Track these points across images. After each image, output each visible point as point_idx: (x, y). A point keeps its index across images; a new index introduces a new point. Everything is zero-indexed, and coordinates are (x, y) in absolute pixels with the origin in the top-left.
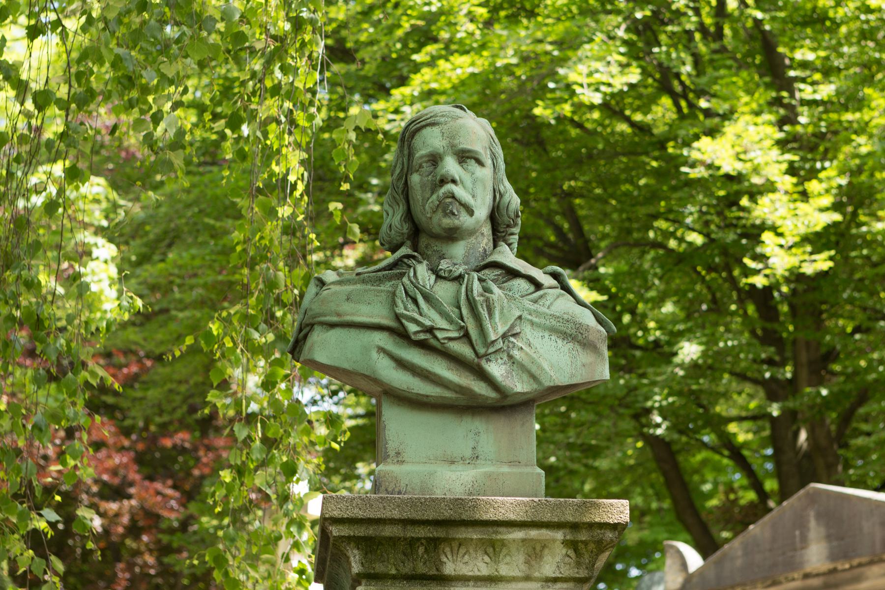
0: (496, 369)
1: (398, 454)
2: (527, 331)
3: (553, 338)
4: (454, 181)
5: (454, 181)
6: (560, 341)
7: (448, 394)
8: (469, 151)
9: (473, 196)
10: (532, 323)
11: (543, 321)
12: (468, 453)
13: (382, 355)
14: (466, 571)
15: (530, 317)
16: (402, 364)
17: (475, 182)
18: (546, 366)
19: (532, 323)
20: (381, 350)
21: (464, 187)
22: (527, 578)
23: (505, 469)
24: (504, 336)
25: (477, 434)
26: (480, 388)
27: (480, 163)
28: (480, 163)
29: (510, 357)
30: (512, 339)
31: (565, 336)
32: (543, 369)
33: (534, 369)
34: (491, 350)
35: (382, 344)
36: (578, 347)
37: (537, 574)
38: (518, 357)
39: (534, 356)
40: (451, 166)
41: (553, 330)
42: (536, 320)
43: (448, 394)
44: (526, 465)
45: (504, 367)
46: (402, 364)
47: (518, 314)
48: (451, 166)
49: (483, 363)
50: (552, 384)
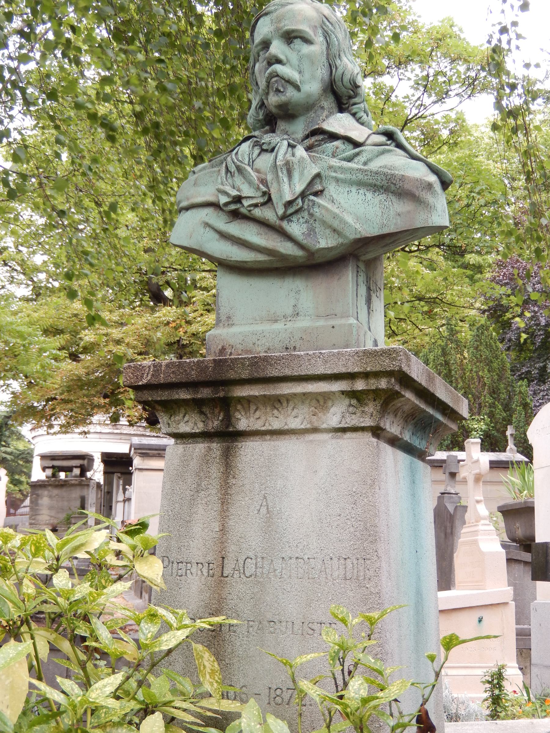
0: (295, 228)
1: (229, 318)
2: (332, 189)
3: (361, 191)
4: (279, 61)
5: (279, 61)
6: (369, 195)
7: (261, 257)
8: (293, 31)
9: (300, 72)
10: (337, 180)
11: (348, 176)
12: (289, 311)
13: (208, 229)
14: (258, 425)
15: (334, 174)
16: (224, 236)
17: (301, 59)
18: (350, 219)
19: (337, 180)
20: (207, 225)
21: (291, 65)
22: (315, 430)
23: (321, 323)
24: (303, 195)
25: (298, 292)
26: (286, 248)
27: (307, 41)
28: (307, 41)
29: (311, 215)
30: (312, 197)
31: (375, 188)
32: (346, 223)
33: (336, 224)
34: (290, 211)
35: (207, 220)
36: (394, 198)
37: (324, 426)
38: (318, 214)
39: (337, 211)
40: (277, 48)
41: (360, 184)
42: (341, 176)
43: (261, 257)
44: (342, 317)
45: (305, 226)
46: (224, 236)
47: (315, 171)
48: (277, 48)
49: (285, 224)
50: (358, 236)
